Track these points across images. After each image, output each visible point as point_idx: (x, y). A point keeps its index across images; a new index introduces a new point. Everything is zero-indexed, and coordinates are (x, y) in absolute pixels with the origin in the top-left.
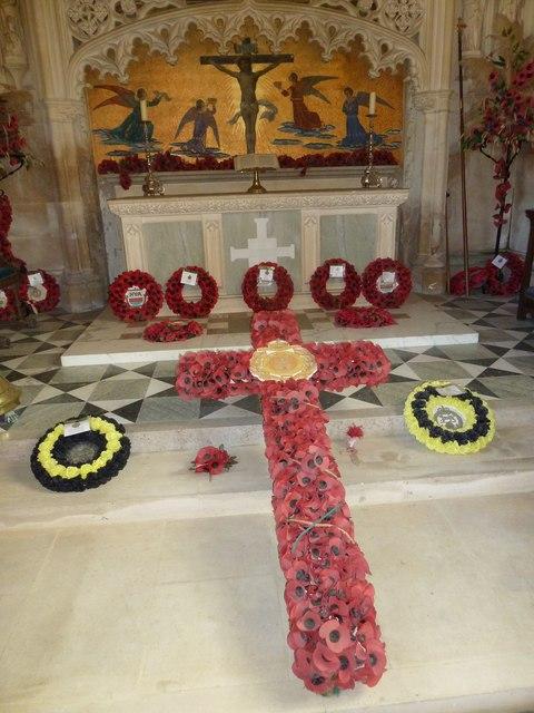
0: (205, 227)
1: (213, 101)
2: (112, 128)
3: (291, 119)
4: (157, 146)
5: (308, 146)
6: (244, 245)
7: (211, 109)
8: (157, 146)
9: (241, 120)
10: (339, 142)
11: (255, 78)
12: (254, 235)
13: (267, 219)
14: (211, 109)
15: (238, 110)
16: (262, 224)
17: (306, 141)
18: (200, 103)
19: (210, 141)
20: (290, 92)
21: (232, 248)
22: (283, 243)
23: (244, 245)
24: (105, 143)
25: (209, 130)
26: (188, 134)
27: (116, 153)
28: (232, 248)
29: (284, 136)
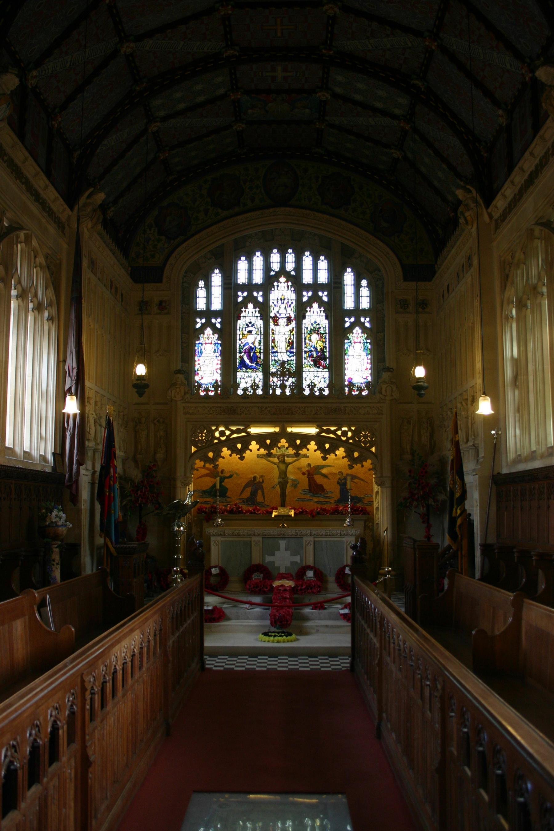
0: (253, 543)
1: (262, 477)
2: (204, 489)
3: (307, 487)
4: (228, 500)
5: (316, 502)
6: (273, 554)
7: (261, 481)
8: (228, 500)
9: (278, 487)
10: (335, 501)
11: (287, 465)
12: (278, 549)
13: (285, 541)
14: (261, 481)
15: (276, 481)
16: (283, 543)
17: (316, 500)
18: (255, 478)
19: (259, 499)
20: (307, 473)
21: (266, 556)
22: (294, 554)
23: (273, 554)
24: (200, 497)
25: (260, 492)
26: (247, 494)
27: (206, 503)
28: (266, 556)
29: (303, 497)
